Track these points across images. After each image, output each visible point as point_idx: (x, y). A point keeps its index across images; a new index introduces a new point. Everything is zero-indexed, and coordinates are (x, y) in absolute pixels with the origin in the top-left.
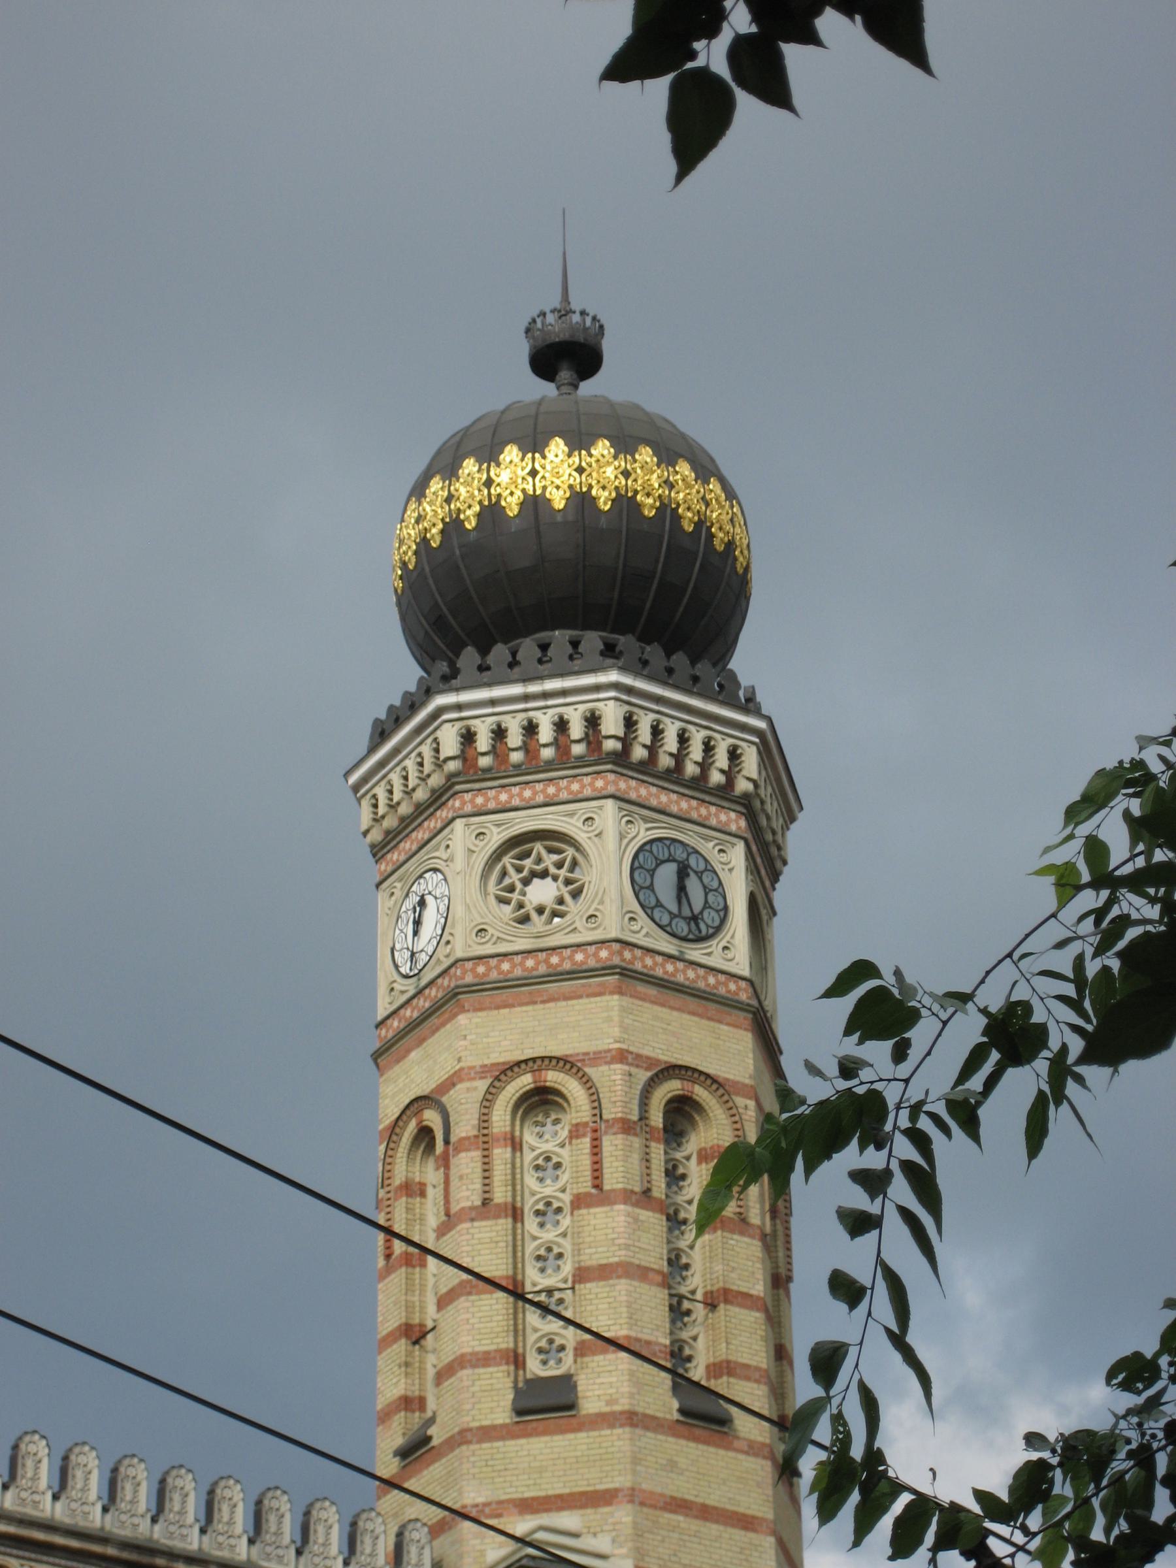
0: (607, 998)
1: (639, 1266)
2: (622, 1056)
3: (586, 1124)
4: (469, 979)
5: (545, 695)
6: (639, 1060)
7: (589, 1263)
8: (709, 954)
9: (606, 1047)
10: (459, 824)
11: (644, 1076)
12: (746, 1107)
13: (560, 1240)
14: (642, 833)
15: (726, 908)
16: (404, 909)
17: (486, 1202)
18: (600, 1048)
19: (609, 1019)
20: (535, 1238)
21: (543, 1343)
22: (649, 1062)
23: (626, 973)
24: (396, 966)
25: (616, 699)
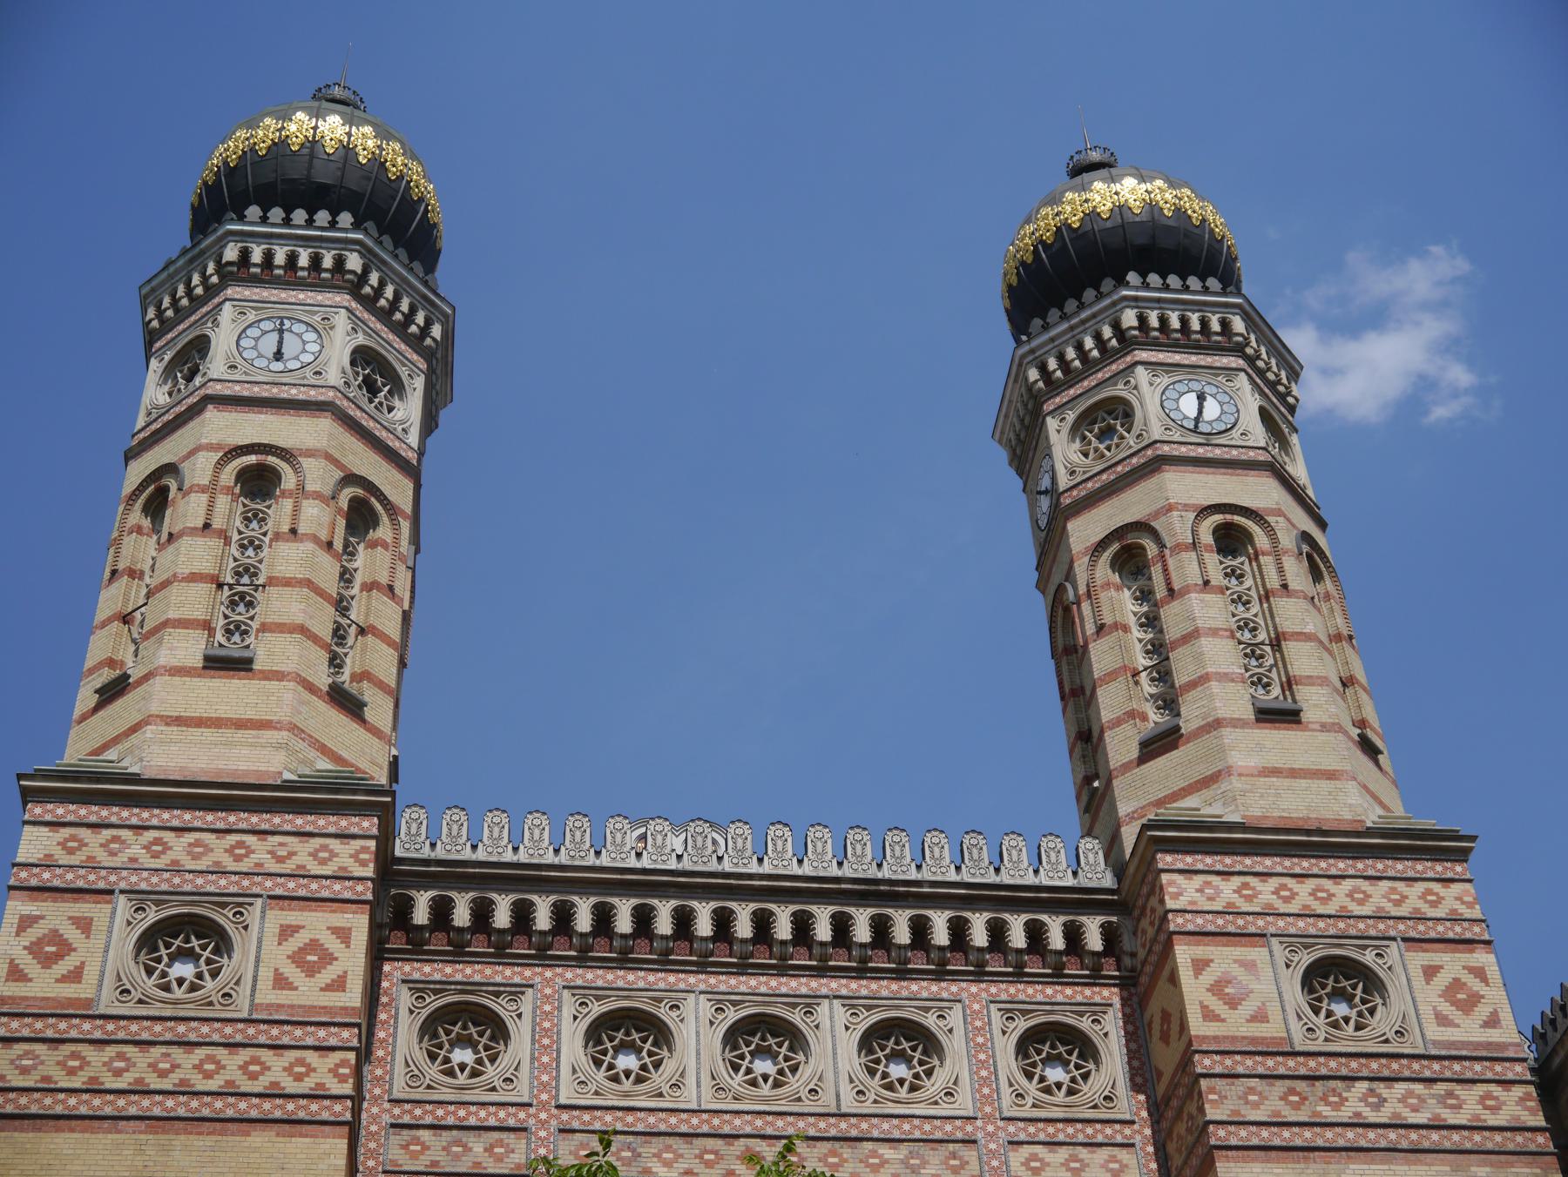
1: (1210, 628)
2: (1170, 508)
5: (1083, 322)
6: (1186, 507)
8: (1232, 439)
11: (1192, 516)
12: (1277, 522)
17: (1100, 629)
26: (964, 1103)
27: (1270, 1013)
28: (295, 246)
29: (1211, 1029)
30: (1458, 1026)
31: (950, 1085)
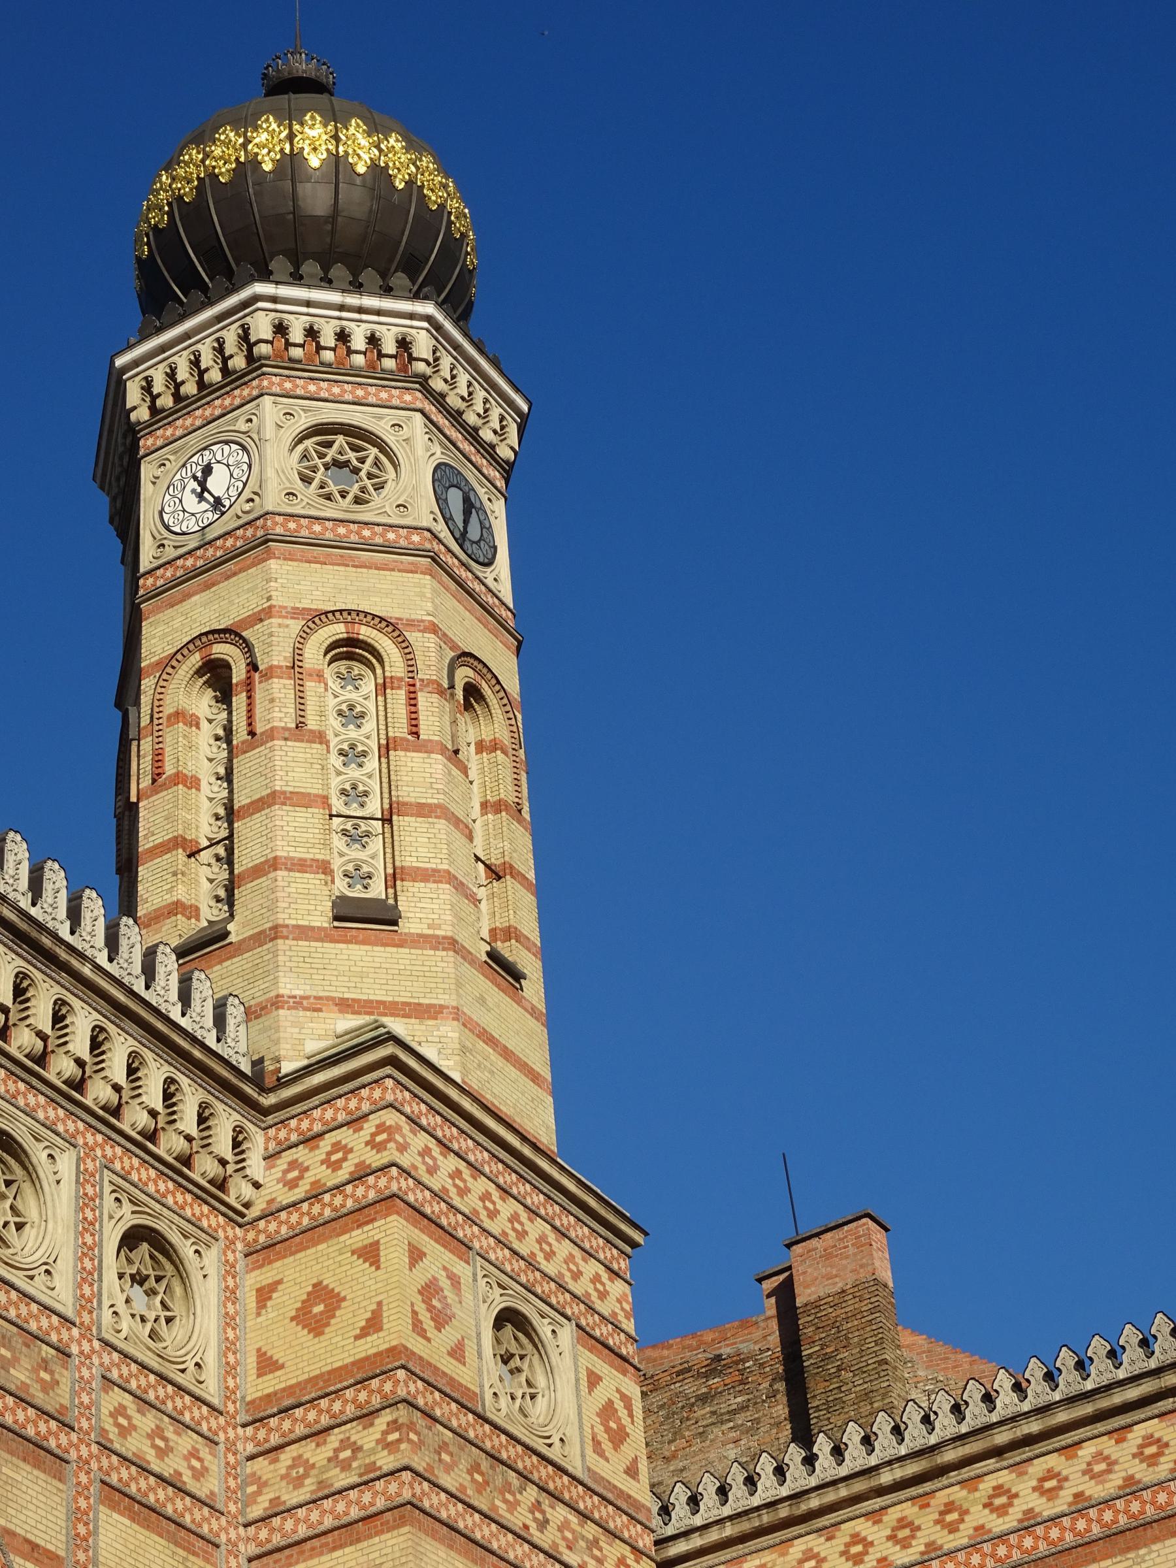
2: (434, 629)
3: (400, 679)
4: (279, 530)
5: (360, 310)
6: (445, 638)
7: (406, 799)
10: (267, 399)
13: (364, 778)
14: (439, 456)
16: (178, 476)
18: (413, 617)
20: (339, 773)
21: (350, 867)
22: (454, 647)
24: (167, 527)
25: (428, 330)
26: (63, 1295)
27: (467, 1354)
29: (417, 1345)
30: (607, 1460)
31: (51, 1261)
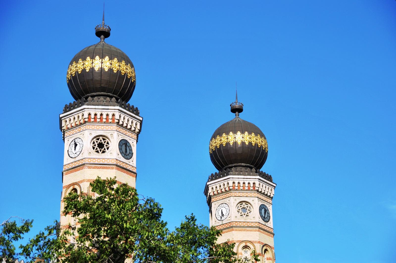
0: (257, 232)
2: (259, 242)
4: (234, 225)
6: (262, 243)
9: (257, 240)
11: (262, 245)
14: (260, 203)
15: (270, 216)
19: (257, 236)
22: (262, 243)
23: (260, 228)
28: (129, 117)
